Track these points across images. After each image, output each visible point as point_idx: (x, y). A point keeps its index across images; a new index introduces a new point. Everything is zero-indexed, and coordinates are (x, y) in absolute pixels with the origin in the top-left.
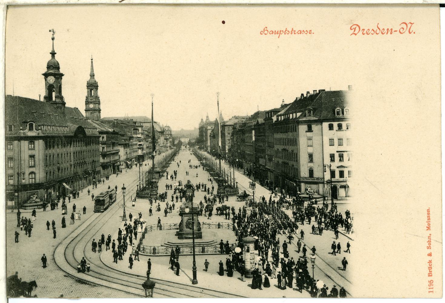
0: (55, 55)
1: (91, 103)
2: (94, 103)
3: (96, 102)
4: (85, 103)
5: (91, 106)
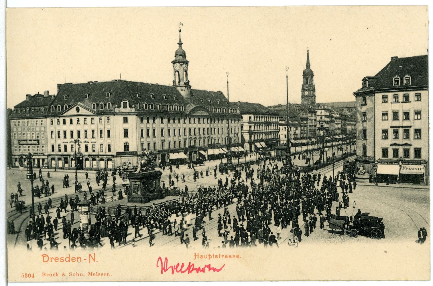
0: (182, 45)
1: (306, 90)
2: (309, 90)
3: (310, 90)
4: (301, 90)
5: (306, 93)
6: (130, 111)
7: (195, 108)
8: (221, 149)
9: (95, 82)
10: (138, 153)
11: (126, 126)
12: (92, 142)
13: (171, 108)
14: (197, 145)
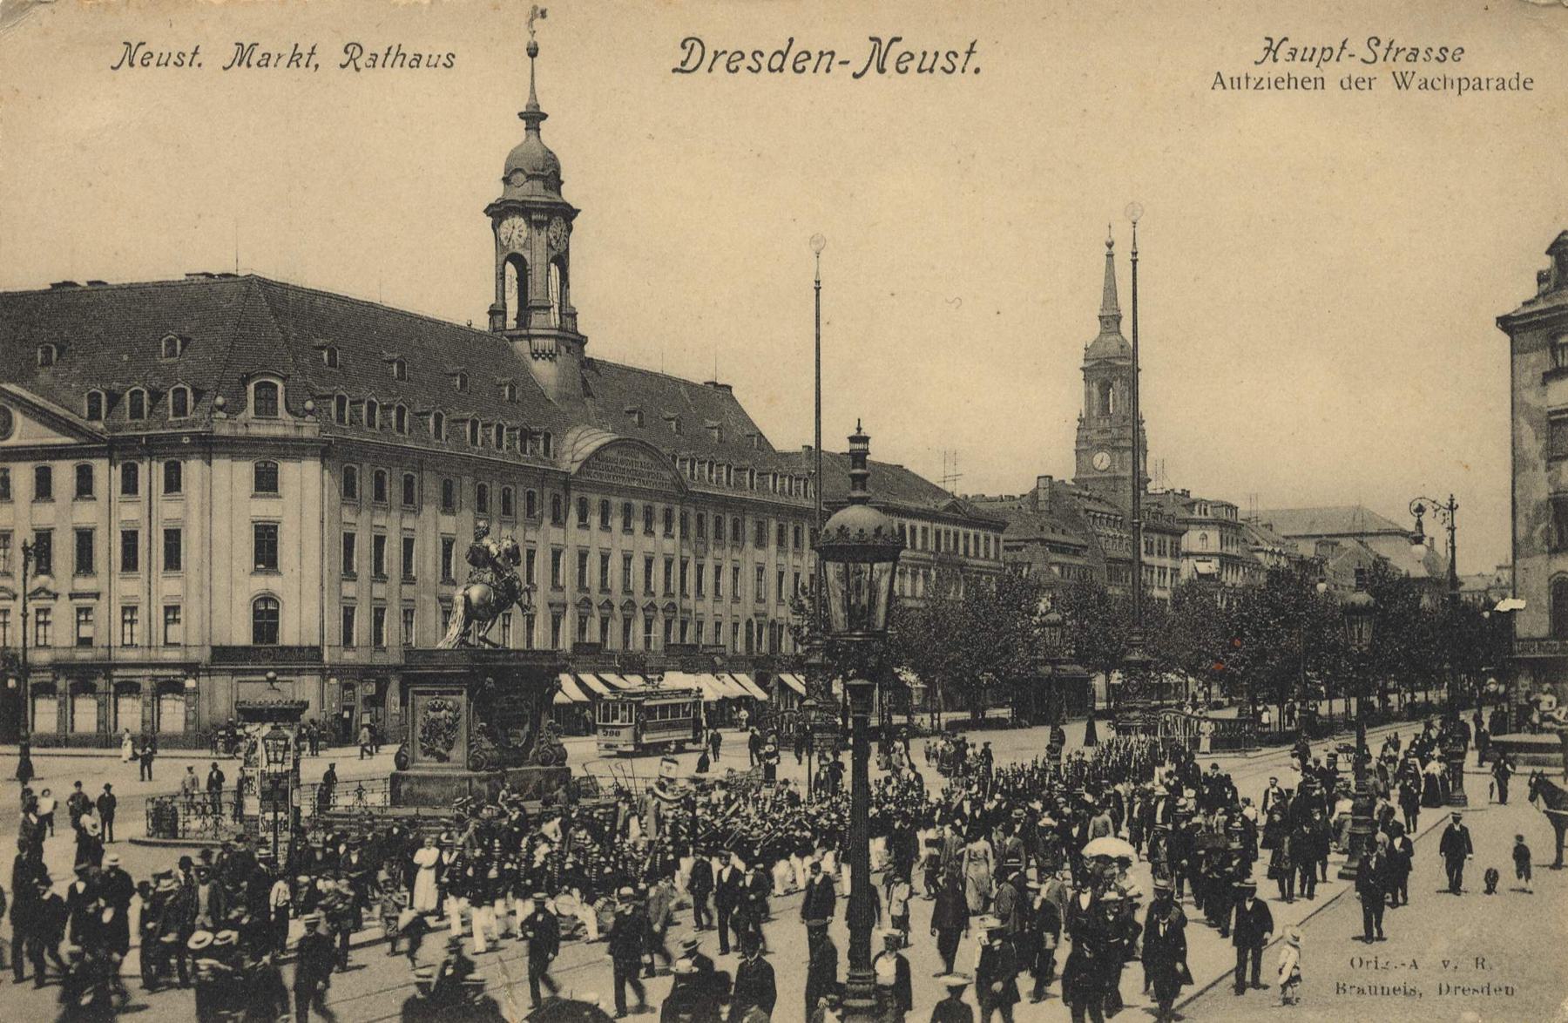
0: (543, 124)
3: (1122, 443)
6: (292, 433)
7: (603, 447)
8: (727, 677)
9: (90, 283)
10: (326, 658)
11: (265, 508)
12: (72, 596)
13: (493, 438)
14: (614, 642)
